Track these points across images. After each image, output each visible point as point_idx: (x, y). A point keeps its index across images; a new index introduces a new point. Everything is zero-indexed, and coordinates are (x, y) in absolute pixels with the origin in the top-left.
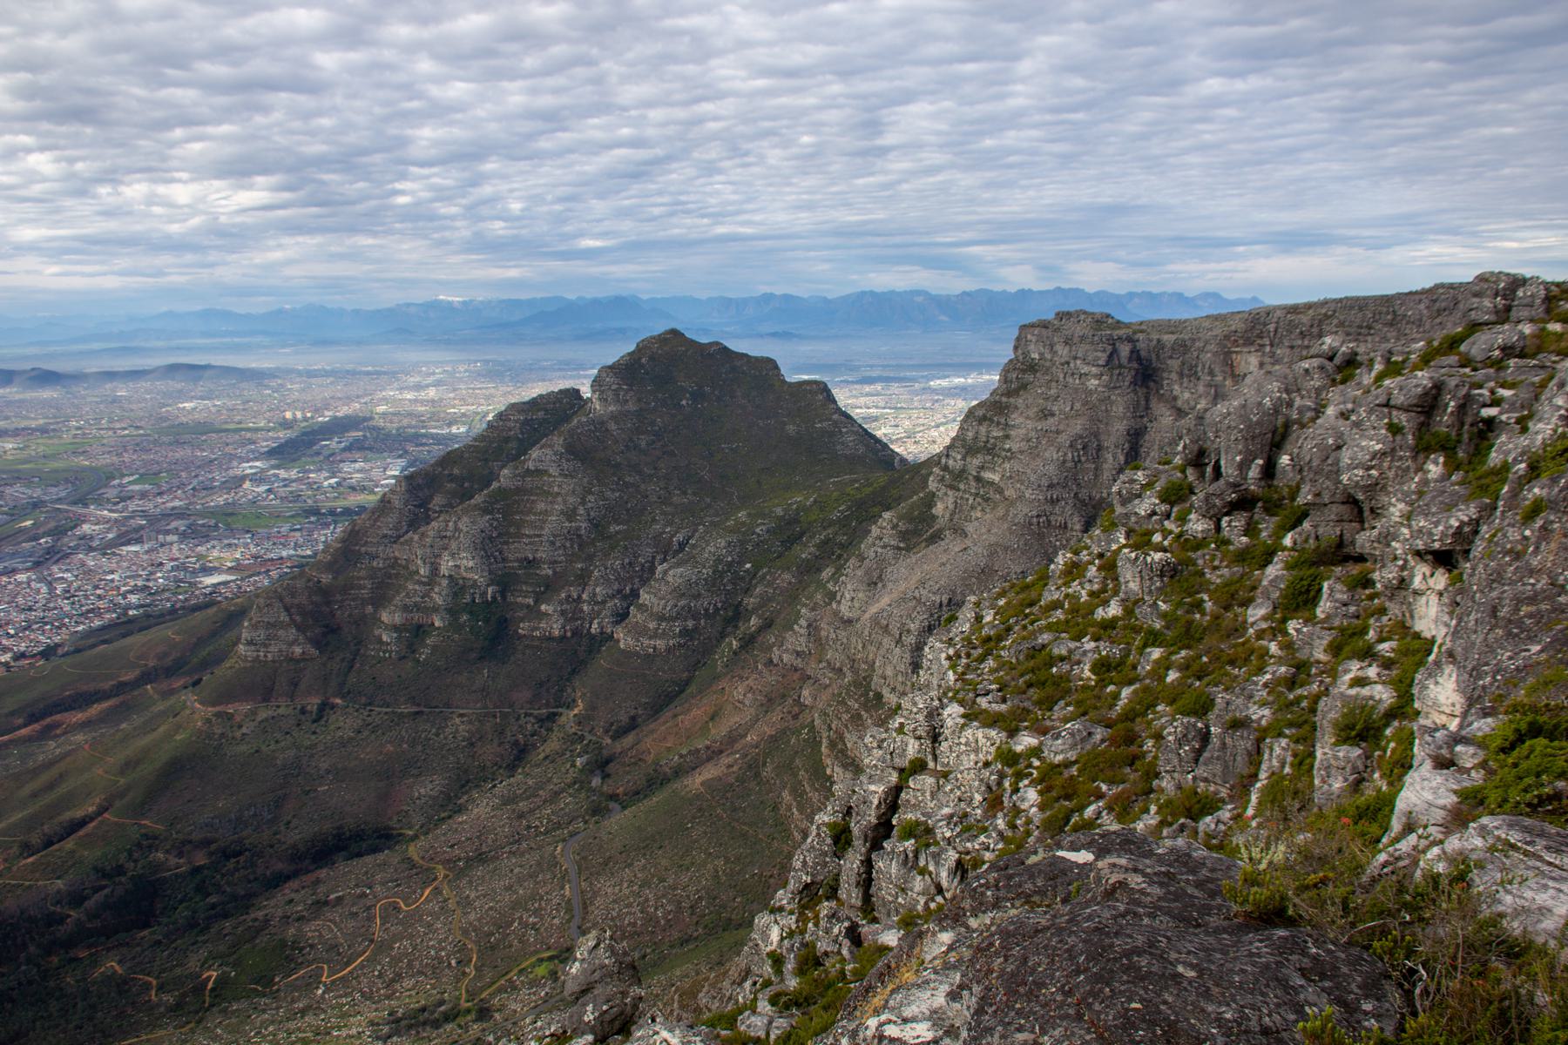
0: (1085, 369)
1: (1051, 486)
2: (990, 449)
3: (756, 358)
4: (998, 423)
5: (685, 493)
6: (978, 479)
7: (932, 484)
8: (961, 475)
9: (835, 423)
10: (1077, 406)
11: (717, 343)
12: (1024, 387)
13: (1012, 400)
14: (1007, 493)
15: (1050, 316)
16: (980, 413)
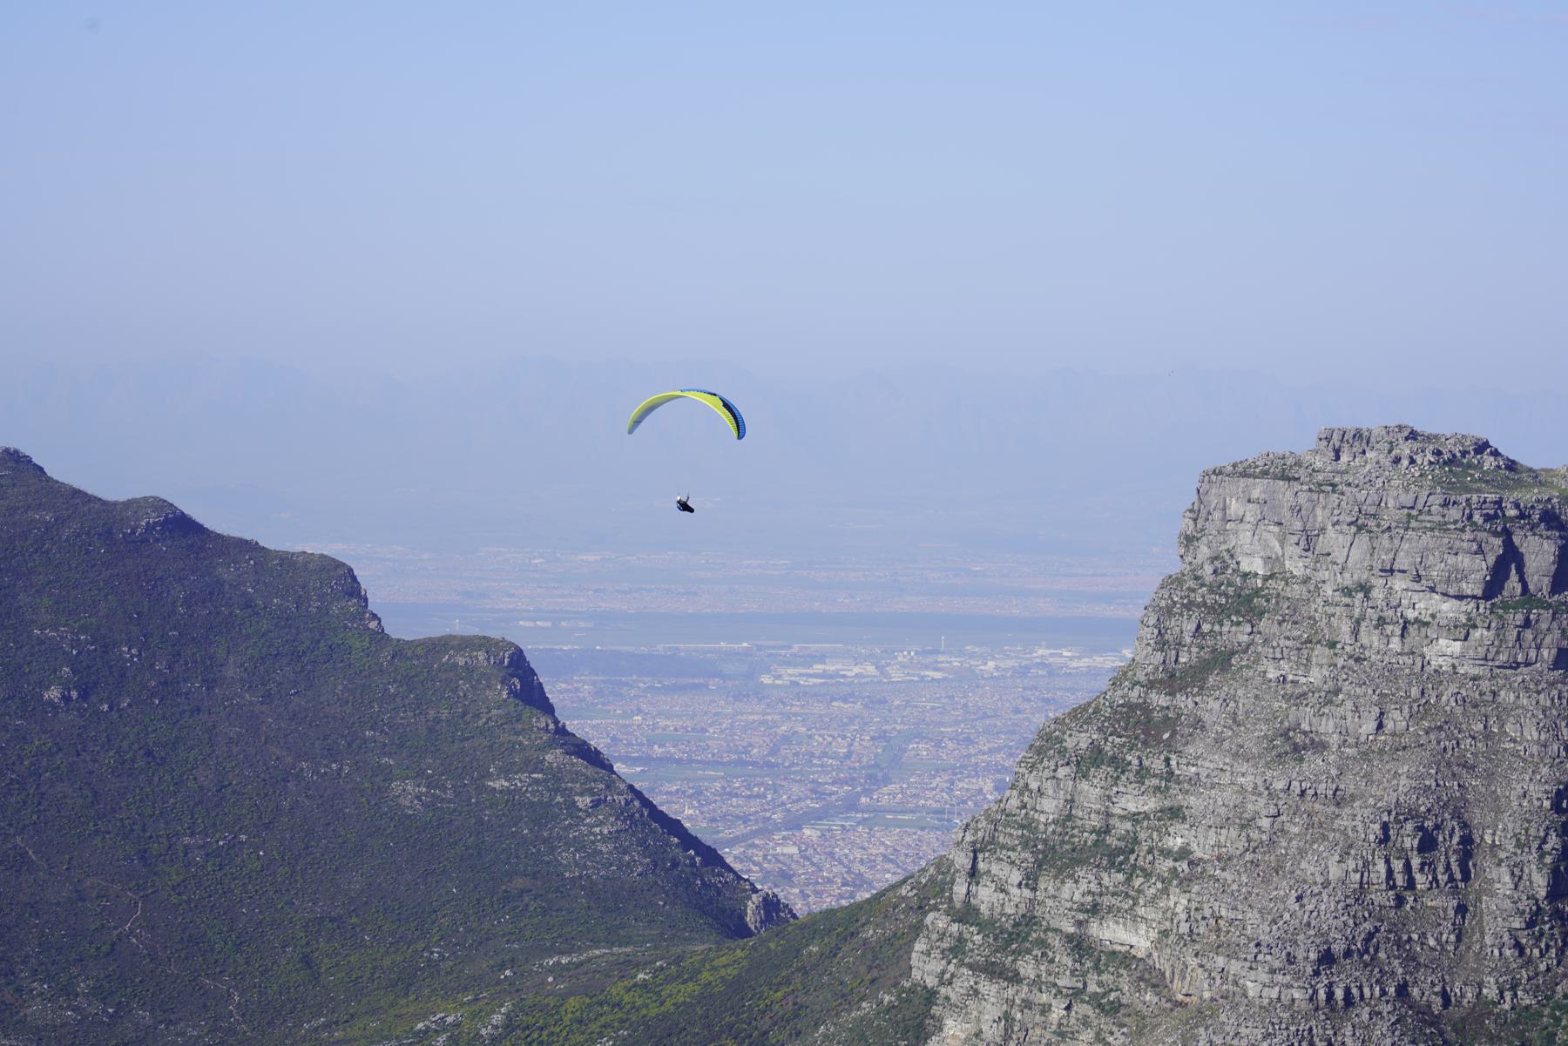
0: (1424, 605)
1: (1327, 958)
2: (1114, 853)
3: (287, 561)
4: (1143, 773)
5: (68, 991)
6: (1080, 946)
7: (925, 967)
8: (1020, 934)
9: (555, 778)
10: (1396, 720)
11: (160, 504)
12: (1221, 660)
13: (1180, 700)
14: (1178, 989)
15: (1300, 442)
16: (1079, 740)
